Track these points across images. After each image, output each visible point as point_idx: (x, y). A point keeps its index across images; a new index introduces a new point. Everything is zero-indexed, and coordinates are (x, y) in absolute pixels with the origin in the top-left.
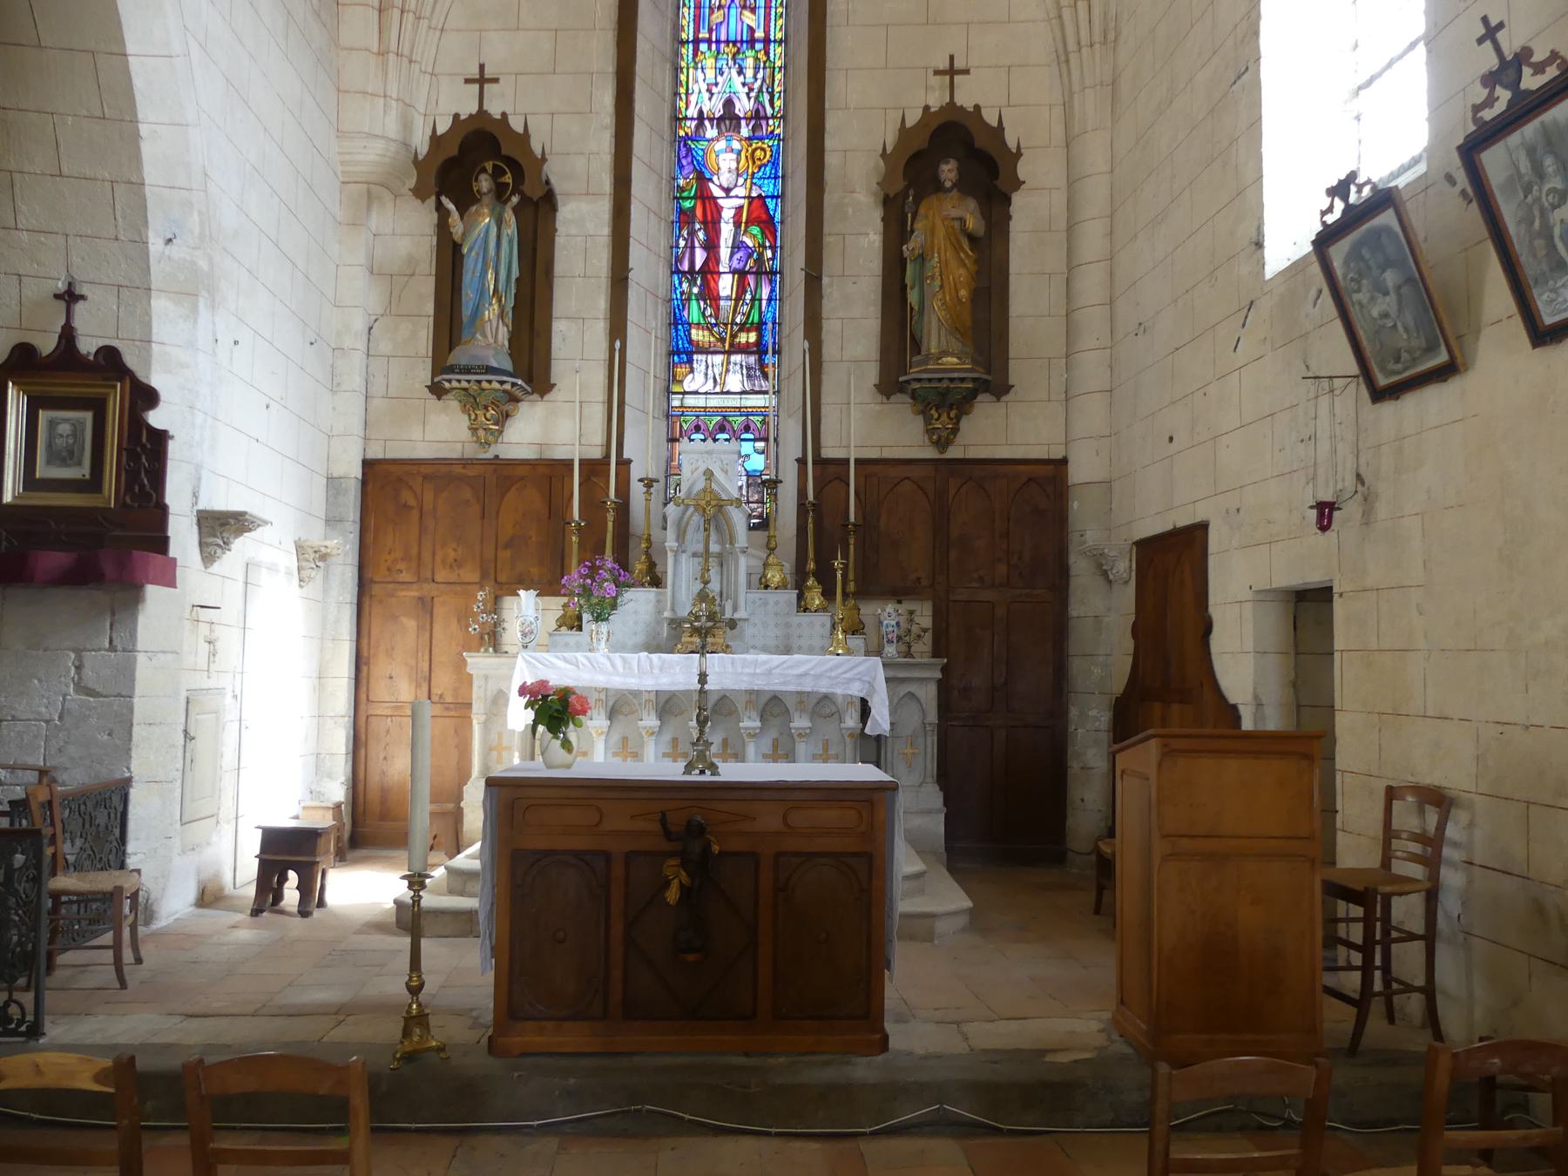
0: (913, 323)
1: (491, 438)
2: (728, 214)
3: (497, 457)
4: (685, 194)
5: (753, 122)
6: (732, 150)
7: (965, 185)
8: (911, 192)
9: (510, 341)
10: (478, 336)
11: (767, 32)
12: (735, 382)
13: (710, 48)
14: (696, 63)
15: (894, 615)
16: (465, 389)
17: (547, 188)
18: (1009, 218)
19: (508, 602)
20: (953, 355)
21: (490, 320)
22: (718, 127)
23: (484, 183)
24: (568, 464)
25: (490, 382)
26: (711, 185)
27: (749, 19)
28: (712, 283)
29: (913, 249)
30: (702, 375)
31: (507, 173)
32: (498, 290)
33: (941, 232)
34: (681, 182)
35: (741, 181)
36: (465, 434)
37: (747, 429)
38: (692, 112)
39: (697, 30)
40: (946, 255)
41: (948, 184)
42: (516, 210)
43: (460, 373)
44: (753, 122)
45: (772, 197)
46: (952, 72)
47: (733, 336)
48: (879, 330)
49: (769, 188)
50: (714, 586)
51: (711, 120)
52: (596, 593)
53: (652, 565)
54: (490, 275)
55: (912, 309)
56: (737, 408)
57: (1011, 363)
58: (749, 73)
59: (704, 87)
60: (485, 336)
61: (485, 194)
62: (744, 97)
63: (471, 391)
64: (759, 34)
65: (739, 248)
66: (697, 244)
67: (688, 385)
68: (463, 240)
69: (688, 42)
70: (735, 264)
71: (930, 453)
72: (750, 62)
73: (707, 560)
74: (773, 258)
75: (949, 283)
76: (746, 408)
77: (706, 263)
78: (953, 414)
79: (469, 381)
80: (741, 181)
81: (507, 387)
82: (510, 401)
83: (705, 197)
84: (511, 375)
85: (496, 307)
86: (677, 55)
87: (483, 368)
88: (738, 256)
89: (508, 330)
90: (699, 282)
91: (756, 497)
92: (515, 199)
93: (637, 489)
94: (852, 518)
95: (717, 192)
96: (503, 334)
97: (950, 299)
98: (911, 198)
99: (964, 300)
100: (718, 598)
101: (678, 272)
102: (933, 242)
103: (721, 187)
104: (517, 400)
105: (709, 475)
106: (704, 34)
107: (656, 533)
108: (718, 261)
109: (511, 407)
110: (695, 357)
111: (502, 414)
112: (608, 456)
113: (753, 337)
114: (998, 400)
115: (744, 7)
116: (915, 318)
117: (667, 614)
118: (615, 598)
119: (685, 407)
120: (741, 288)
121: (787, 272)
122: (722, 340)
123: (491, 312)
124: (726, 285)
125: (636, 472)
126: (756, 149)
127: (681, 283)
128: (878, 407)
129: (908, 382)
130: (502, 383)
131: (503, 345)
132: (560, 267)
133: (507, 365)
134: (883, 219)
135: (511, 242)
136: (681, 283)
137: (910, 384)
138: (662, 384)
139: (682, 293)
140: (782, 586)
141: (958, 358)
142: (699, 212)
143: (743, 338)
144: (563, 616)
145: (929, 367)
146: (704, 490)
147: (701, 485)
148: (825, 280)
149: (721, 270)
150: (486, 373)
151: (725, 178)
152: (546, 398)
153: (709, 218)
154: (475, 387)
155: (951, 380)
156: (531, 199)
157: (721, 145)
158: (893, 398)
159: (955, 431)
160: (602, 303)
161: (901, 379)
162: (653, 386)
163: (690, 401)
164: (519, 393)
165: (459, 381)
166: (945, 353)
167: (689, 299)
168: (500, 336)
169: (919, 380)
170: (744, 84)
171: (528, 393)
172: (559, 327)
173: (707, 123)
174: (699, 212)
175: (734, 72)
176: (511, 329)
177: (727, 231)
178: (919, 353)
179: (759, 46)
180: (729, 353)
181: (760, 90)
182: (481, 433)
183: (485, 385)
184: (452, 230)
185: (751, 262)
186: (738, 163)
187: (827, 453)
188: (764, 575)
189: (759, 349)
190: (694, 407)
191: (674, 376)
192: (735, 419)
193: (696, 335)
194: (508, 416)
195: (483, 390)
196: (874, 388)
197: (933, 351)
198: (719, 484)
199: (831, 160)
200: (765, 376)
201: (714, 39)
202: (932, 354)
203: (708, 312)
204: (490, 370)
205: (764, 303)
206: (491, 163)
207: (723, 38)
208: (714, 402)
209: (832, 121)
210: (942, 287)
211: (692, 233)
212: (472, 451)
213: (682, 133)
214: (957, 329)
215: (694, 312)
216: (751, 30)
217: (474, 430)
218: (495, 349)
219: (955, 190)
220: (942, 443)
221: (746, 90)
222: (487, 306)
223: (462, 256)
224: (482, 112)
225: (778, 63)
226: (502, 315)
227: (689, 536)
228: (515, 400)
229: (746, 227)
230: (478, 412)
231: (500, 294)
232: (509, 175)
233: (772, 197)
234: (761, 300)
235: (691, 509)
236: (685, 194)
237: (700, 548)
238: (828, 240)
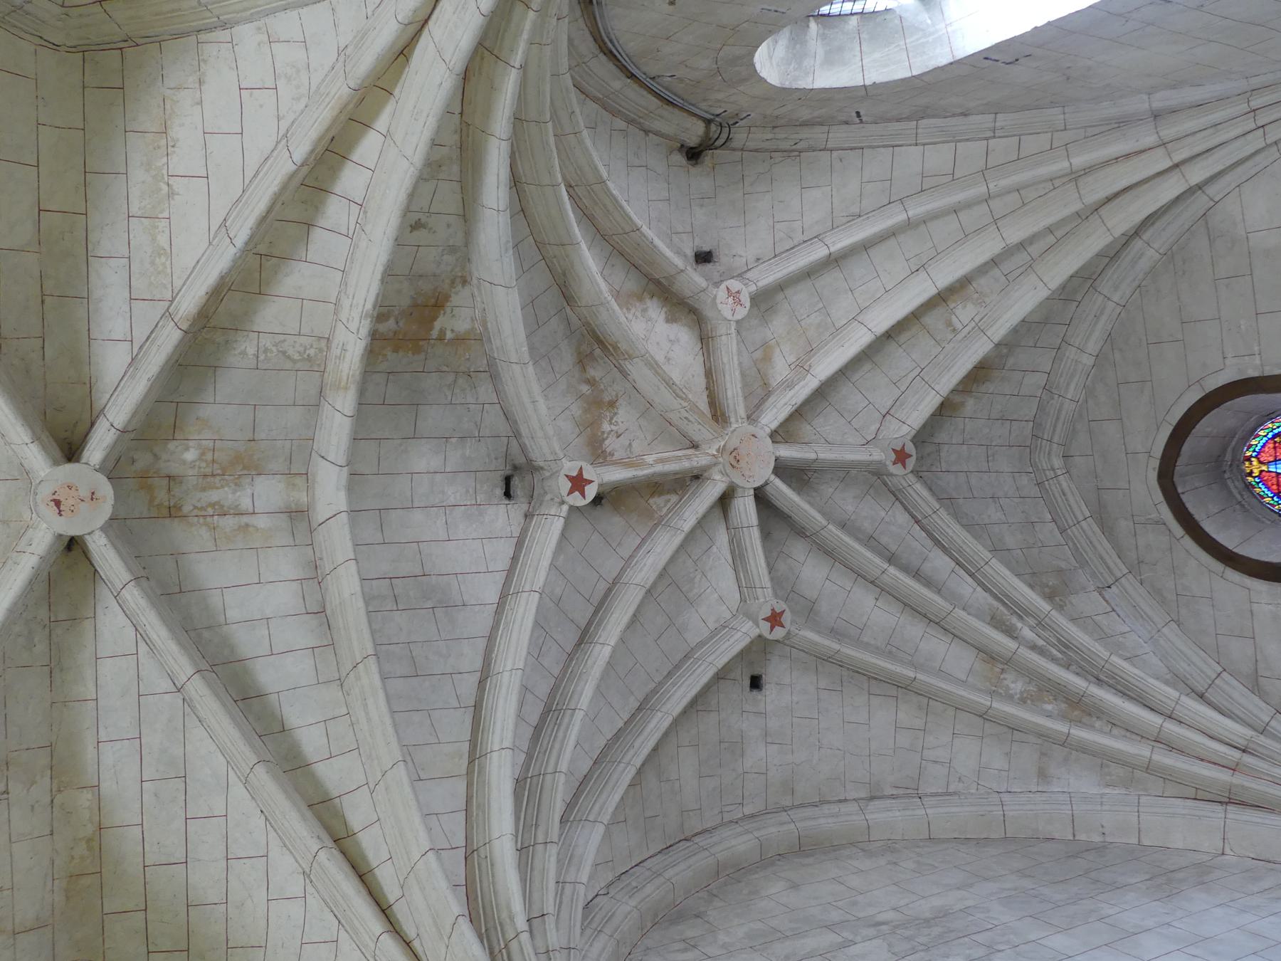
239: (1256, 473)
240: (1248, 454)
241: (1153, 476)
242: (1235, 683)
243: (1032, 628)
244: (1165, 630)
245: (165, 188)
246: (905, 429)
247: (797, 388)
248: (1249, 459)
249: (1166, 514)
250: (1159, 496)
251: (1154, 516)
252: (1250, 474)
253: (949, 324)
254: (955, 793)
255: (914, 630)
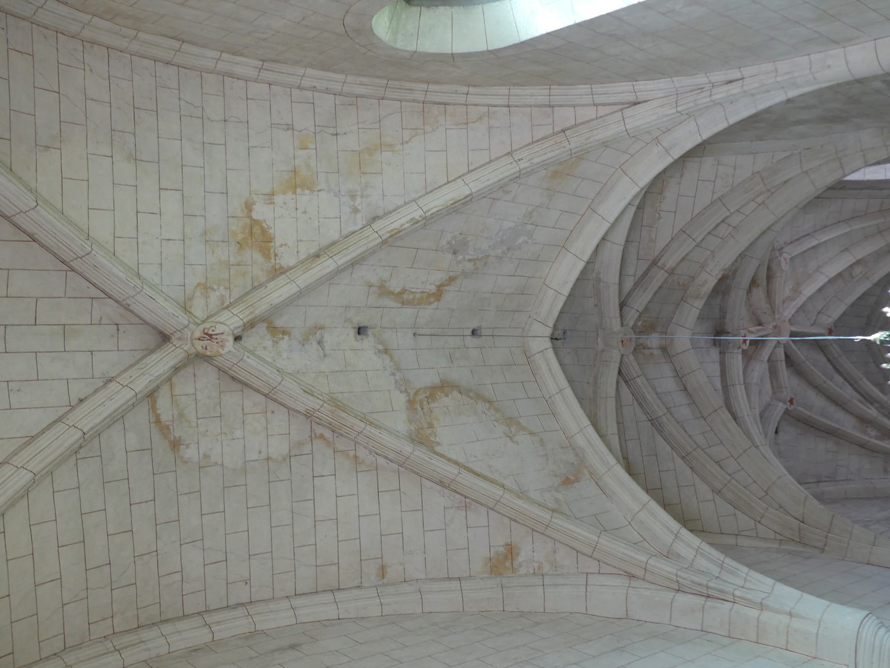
243: (876, 408)
245: (658, 215)
246: (831, 320)
247: (797, 300)
253: (851, 274)
254: (850, 480)
255: (832, 408)
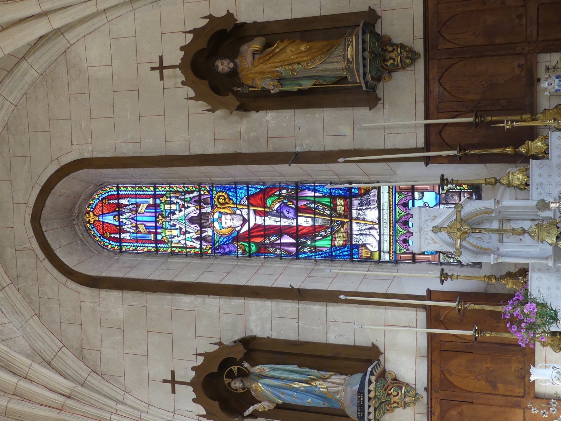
0: (325, 83)
1: (412, 393)
2: (259, 221)
3: (426, 389)
4: (247, 249)
5: (202, 204)
6: (220, 218)
7: (233, 55)
8: (235, 89)
9: (342, 374)
10: (338, 397)
11: (149, 197)
12: (372, 215)
13: (160, 233)
14: (169, 242)
15: (550, 81)
16: (375, 409)
17: (238, 343)
18: (255, 23)
19: (540, 388)
20: (346, 51)
21: (327, 388)
22: (206, 227)
23: (237, 385)
24: (431, 337)
25: (369, 391)
26: (241, 232)
27: (142, 208)
28: (304, 231)
29: (274, 86)
30: (367, 238)
31: (231, 369)
32: (305, 381)
33: (261, 67)
34: (240, 252)
35: (238, 212)
36: (409, 411)
37: (405, 205)
38: (197, 244)
39: (150, 241)
40: (277, 62)
41: (231, 65)
42: (253, 365)
43: (363, 412)
44: (202, 204)
45: (248, 190)
46: (161, 68)
47: (340, 216)
48: (330, 109)
49: (242, 193)
50: (527, 225)
51: (201, 233)
52: (533, 319)
53: (509, 275)
54: (296, 385)
55: (314, 85)
56: (390, 213)
57: (353, 10)
58: (174, 207)
59: (182, 237)
60: (338, 392)
61: (244, 385)
62: (188, 211)
63: (377, 405)
64: (151, 201)
65: (281, 212)
66: (279, 242)
67: (374, 247)
68: (273, 402)
69: (156, 247)
70: (291, 215)
71: (420, 65)
72: (167, 207)
73: (506, 231)
74: (287, 189)
75: (296, 58)
76: (390, 206)
77: (291, 236)
78: (390, 49)
79: (369, 407)
80: (238, 212)
81: (373, 378)
82: (384, 378)
83: (249, 236)
84: (365, 375)
85: (318, 383)
86: (164, 254)
87: (360, 395)
88: (286, 213)
89: (334, 375)
90: (304, 240)
91: (456, 197)
92: (246, 365)
93: (449, 286)
94: (471, 119)
95: (245, 228)
96: (337, 379)
97: (307, 57)
98: (239, 89)
99: (308, 47)
100: (536, 223)
101: (297, 255)
102: (269, 72)
103: (242, 226)
104: (384, 371)
105: (437, 229)
106: (152, 237)
107: (485, 271)
108: (290, 227)
109: (389, 376)
110: (354, 243)
111: (394, 383)
112: (424, 307)
113: (340, 202)
114: (380, 17)
115: (136, 211)
116: (321, 81)
117: (550, 263)
118: (538, 304)
119: (390, 250)
120: (307, 210)
121: (296, 179)
122: (343, 223)
123: (321, 386)
124: (305, 221)
125: (436, 286)
126: (219, 202)
127: (305, 253)
128: (387, 106)
129: (366, 83)
130: (370, 382)
131: (344, 379)
132: (292, 337)
133: (358, 377)
134: (258, 111)
135: (274, 370)
136: (305, 253)
137: (368, 82)
138: (373, 266)
139: (311, 252)
140: (526, 172)
141: (348, 47)
142: (259, 240)
143: (341, 209)
144: (552, 346)
145: (355, 68)
146: (449, 233)
147: (444, 236)
148: (298, 149)
149: (295, 224)
150: (363, 393)
151: (237, 222)
152: (382, 351)
153: (262, 233)
154: (373, 402)
155: (364, 50)
156: (245, 354)
157: (216, 225)
158: (380, 95)
159: (402, 46)
160: (316, 308)
161: (364, 88)
162: (375, 272)
163: (385, 246)
164: (379, 371)
165: (369, 413)
166: (345, 57)
167: (315, 247)
168: (338, 381)
169: (365, 74)
170: (180, 211)
171: (378, 363)
172: (333, 338)
173: (203, 235)
174: (259, 240)
175: (174, 217)
176: (333, 373)
177: (270, 221)
178: (346, 78)
179: (158, 201)
180: (351, 219)
181: (183, 200)
182: (408, 400)
183: (372, 395)
184: (267, 410)
185: (290, 204)
186: (227, 214)
187: (421, 143)
188: (517, 187)
189: (348, 195)
190: (390, 244)
191: (368, 258)
192: (398, 214)
193: (339, 242)
194: (395, 379)
195: (375, 396)
196: (372, 111)
197: (343, 66)
198: (443, 223)
199: (221, 149)
200: (368, 191)
201: (154, 231)
202: (346, 66)
203: (323, 233)
204: (361, 391)
205: (316, 194)
206: (225, 379)
207: (153, 225)
208: (386, 229)
209: (197, 150)
210: (299, 63)
211: (272, 244)
212: (422, 407)
213: (210, 251)
214: (328, 50)
215: (324, 243)
216: (149, 206)
217: (405, 405)
218: (347, 385)
219: (236, 61)
220: (412, 55)
221: (183, 209)
222: (316, 389)
223: (284, 403)
224: (192, 384)
225: (168, 188)
226: (324, 379)
227: (485, 245)
228: (383, 373)
229: (267, 208)
230: (392, 401)
231: (309, 380)
232: (232, 368)
233: (248, 190)
234: (315, 197)
235: (464, 243)
236: (247, 249)
237: (495, 236)
238: (271, 149)
239: (92, 222)
240: (88, 209)
241: (28, 218)
242: (69, 353)
244: (31, 321)
248: (88, 213)
249: (35, 245)
250: (31, 233)
251: (28, 245)
252: (89, 222)
